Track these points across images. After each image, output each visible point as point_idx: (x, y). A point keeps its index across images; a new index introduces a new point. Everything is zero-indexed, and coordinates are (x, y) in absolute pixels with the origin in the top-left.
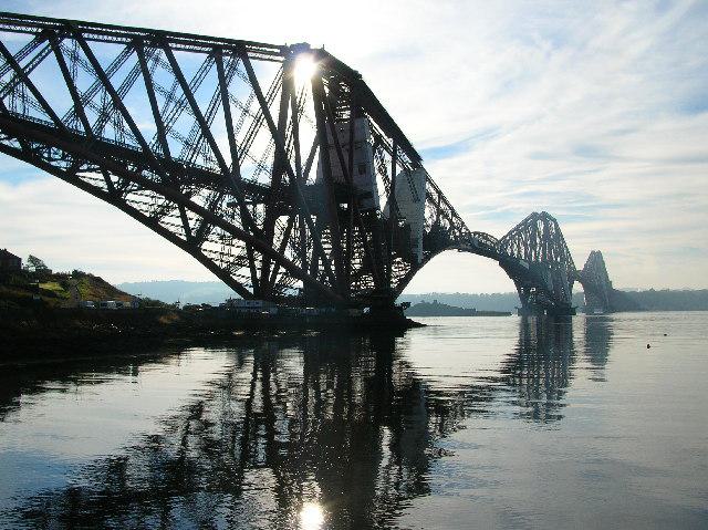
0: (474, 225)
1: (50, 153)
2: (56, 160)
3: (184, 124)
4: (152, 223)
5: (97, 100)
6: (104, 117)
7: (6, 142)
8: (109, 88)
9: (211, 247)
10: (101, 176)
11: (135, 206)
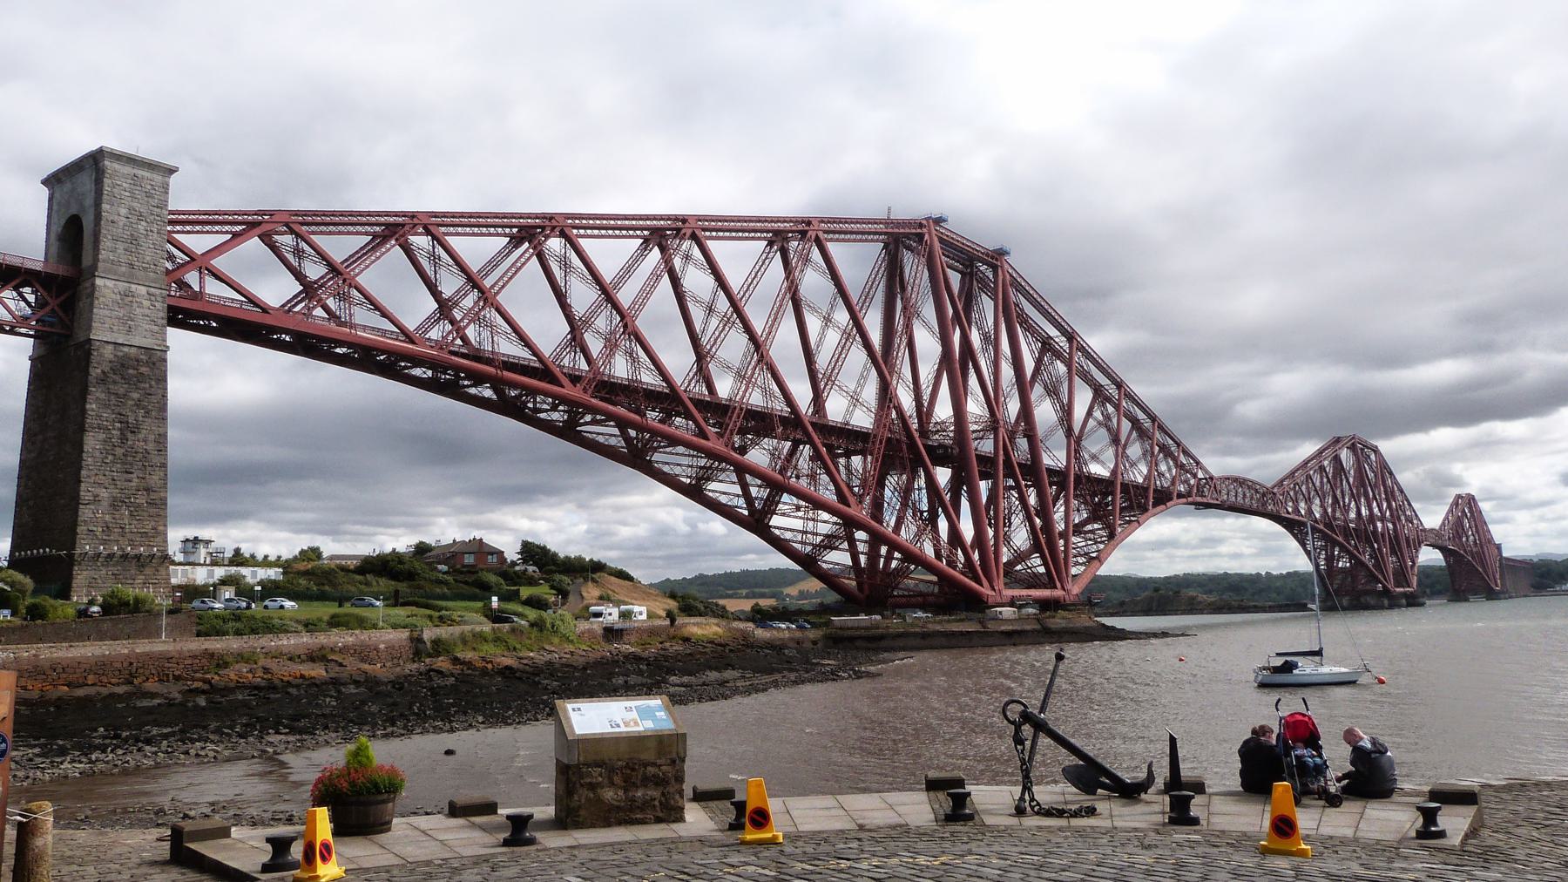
0: (1217, 464)
1: (535, 402)
2: (546, 411)
3: (734, 347)
4: (695, 492)
5: (601, 323)
6: (611, 345)
7: (473, 391)
8: (616, 306)
9: (787, 520)
10: (616, 431)
11: (666, 469)
